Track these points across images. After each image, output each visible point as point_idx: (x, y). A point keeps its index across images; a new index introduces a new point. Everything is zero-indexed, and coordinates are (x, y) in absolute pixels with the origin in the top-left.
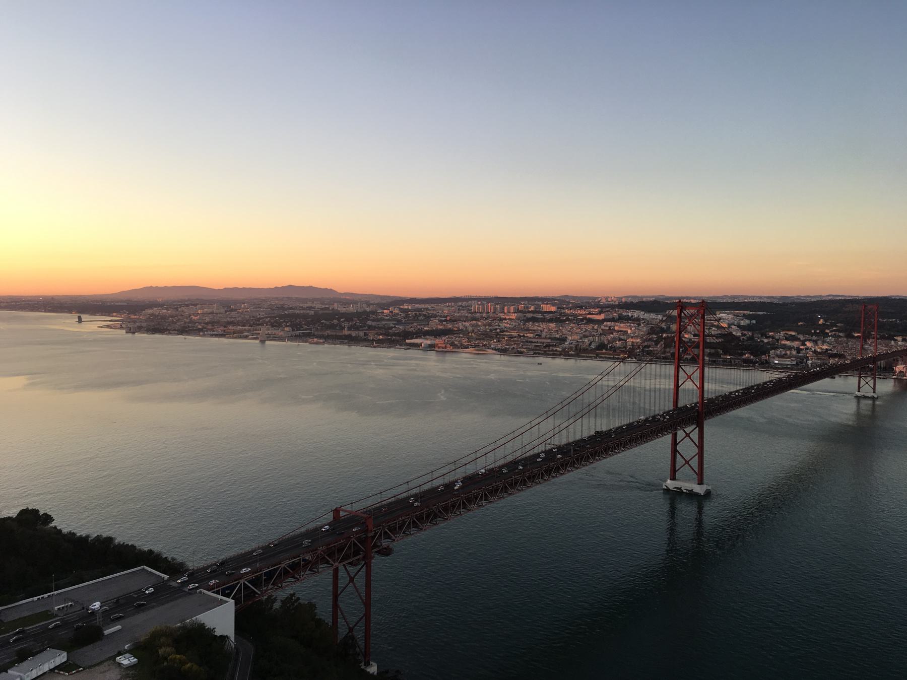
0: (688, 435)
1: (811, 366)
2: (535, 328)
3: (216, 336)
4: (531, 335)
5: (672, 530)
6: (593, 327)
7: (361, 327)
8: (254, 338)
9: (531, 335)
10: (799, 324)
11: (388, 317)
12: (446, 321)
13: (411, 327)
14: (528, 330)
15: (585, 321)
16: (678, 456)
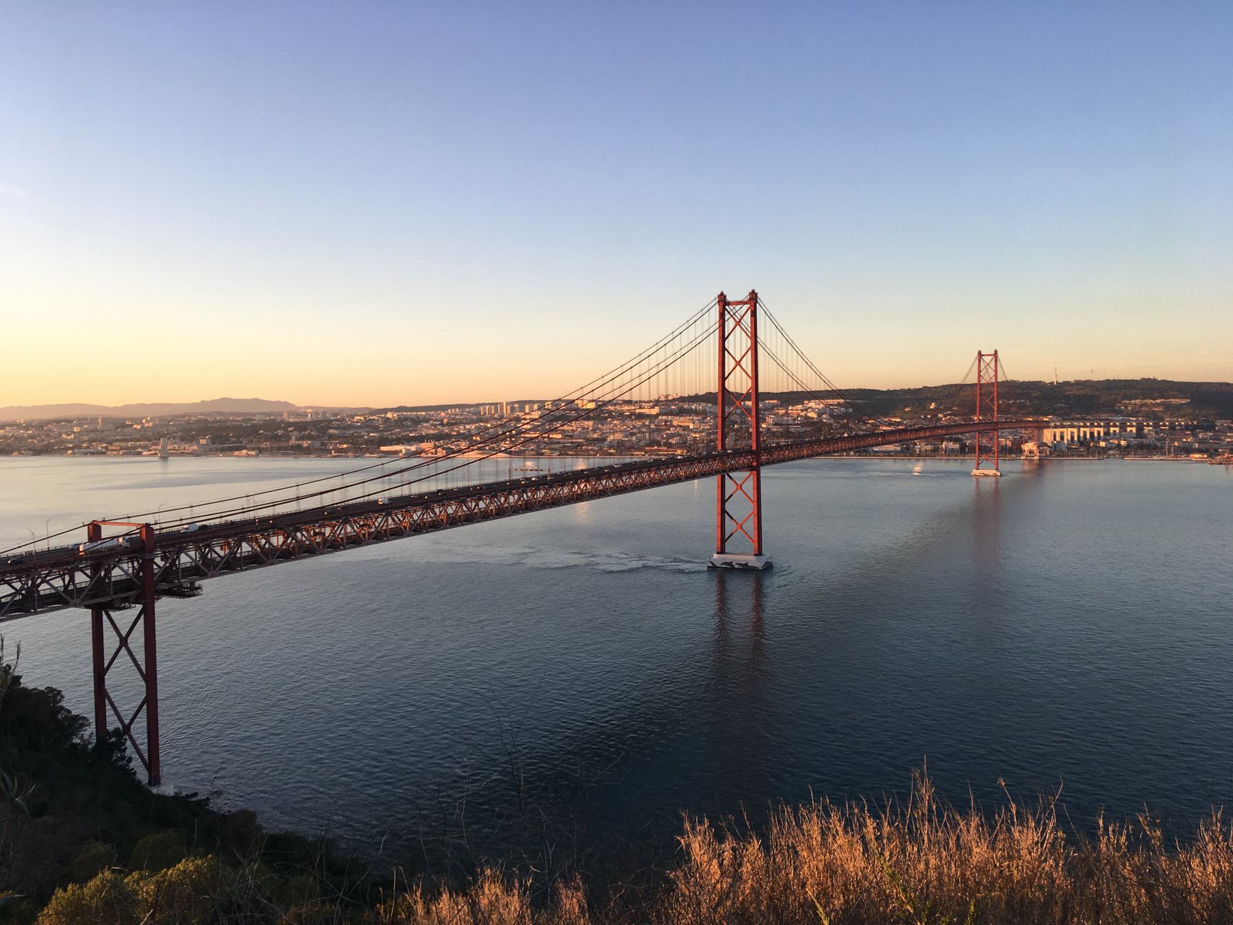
1: (920, 451)
2: (566, 428)
3: (92, 454)
4: (560, 436)
5: (722, 627)
6: (644, 423)
7: (317, 436)
8: (151, 454)
9: (560, 436)
10: (906, 410)
11: (359, 424)
12: (442, 424)
13: (392, 434)
14: (555, 430)
15: (633, 417)
16: (726, 516)
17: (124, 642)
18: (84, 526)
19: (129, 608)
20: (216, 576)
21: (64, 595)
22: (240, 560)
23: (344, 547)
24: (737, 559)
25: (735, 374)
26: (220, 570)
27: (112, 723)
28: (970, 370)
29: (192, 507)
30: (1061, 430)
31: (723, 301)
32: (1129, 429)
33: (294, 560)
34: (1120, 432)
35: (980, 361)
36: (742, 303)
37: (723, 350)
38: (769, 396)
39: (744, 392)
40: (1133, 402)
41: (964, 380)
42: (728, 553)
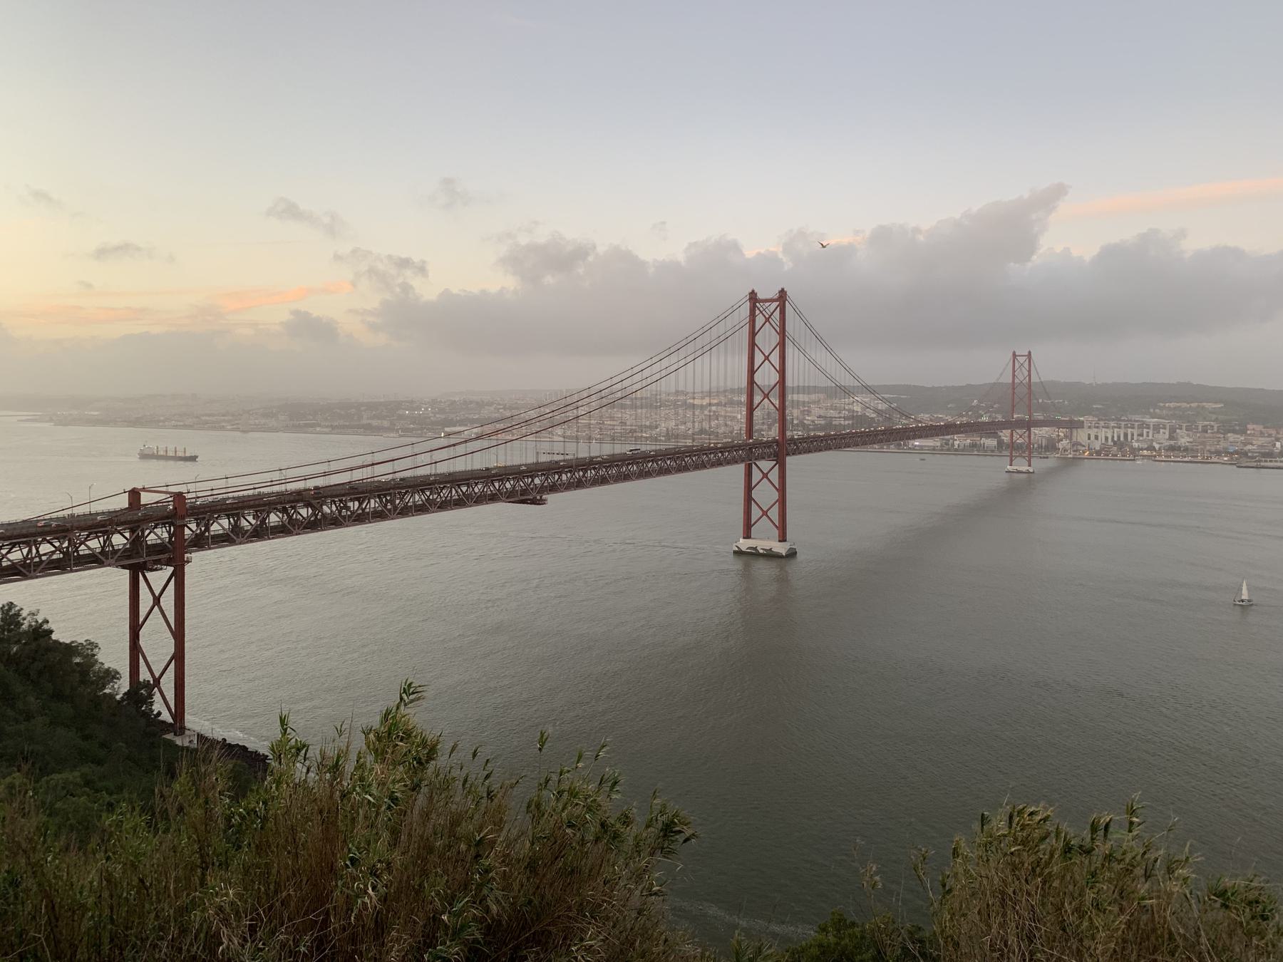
0: (765, 476)
17: (157, 600)
18: (125, 492)
19: (161, 569)
20: (243, 544)
21: (100, 556)
22: (267, 530)
23: (369, 520)
24: (762, 544)
25: (764, 367)
26: (248, 537)
27: (144, 675)
28: (1004, 370)
29: (227, 478)
30: (1096, 430)
31: (753, 297)
32: (1162, 431)
33: (319, 531)
34: (1153, 434)
35: (1014, 361)
36: (772, 300)
37: (752, 345)
38: (799, 390)
39: (773, 383)
40: (1167, 405)
41: (998, 379)
42: (754, 539)
